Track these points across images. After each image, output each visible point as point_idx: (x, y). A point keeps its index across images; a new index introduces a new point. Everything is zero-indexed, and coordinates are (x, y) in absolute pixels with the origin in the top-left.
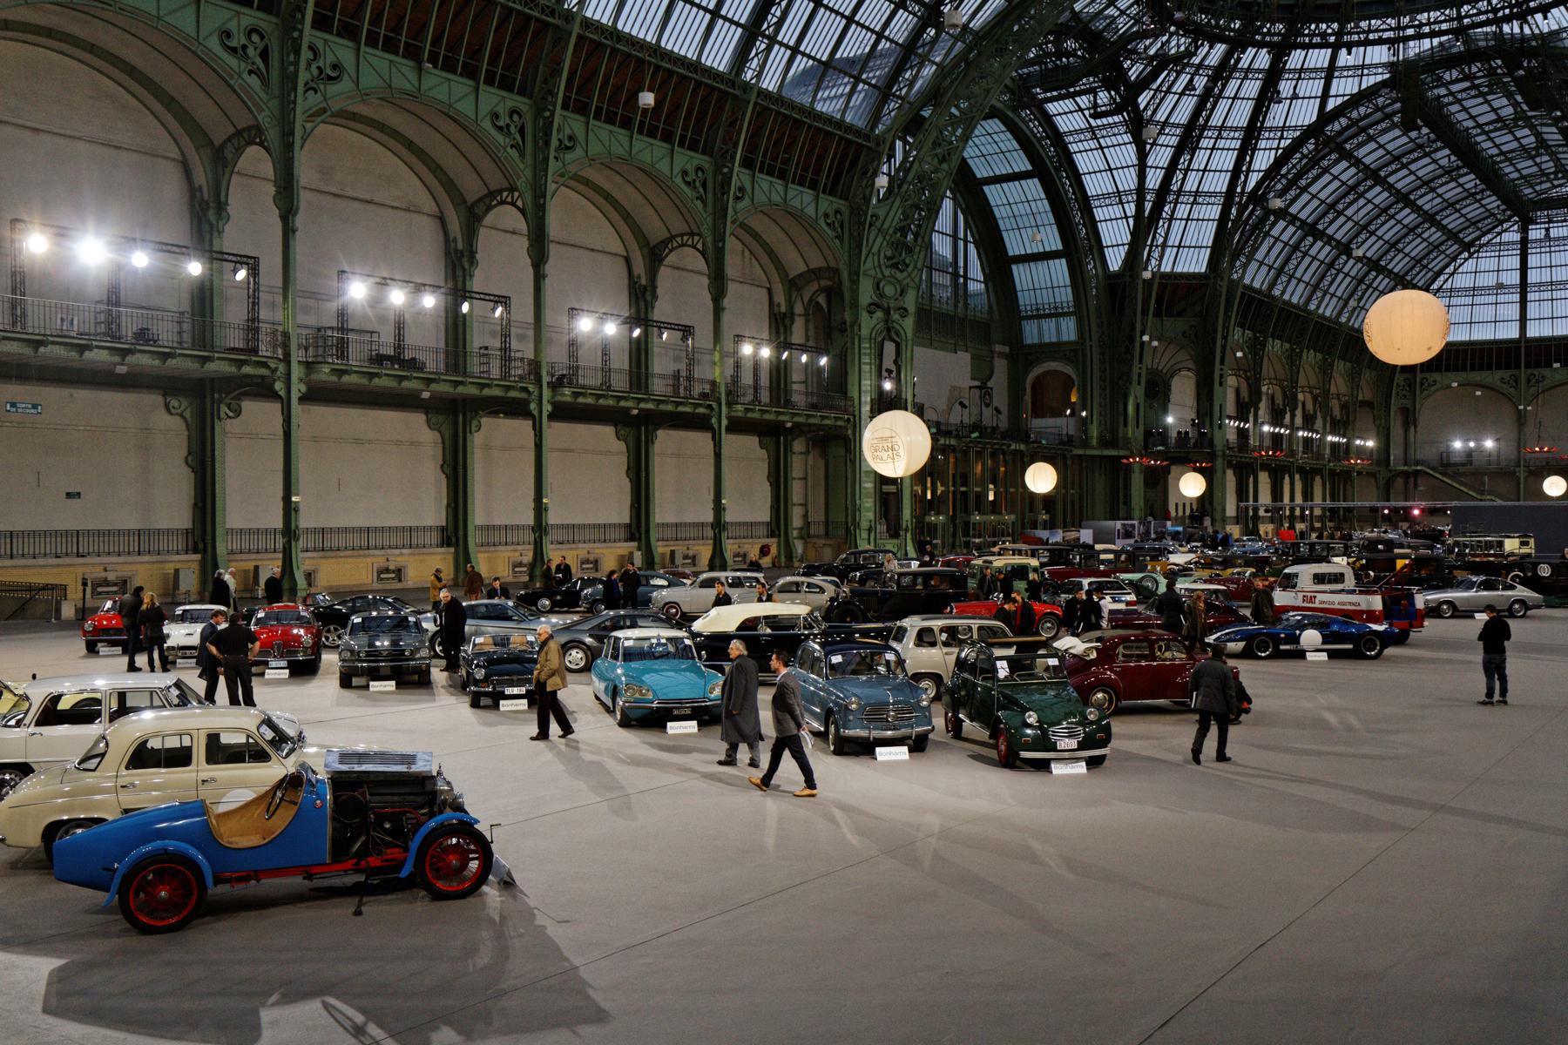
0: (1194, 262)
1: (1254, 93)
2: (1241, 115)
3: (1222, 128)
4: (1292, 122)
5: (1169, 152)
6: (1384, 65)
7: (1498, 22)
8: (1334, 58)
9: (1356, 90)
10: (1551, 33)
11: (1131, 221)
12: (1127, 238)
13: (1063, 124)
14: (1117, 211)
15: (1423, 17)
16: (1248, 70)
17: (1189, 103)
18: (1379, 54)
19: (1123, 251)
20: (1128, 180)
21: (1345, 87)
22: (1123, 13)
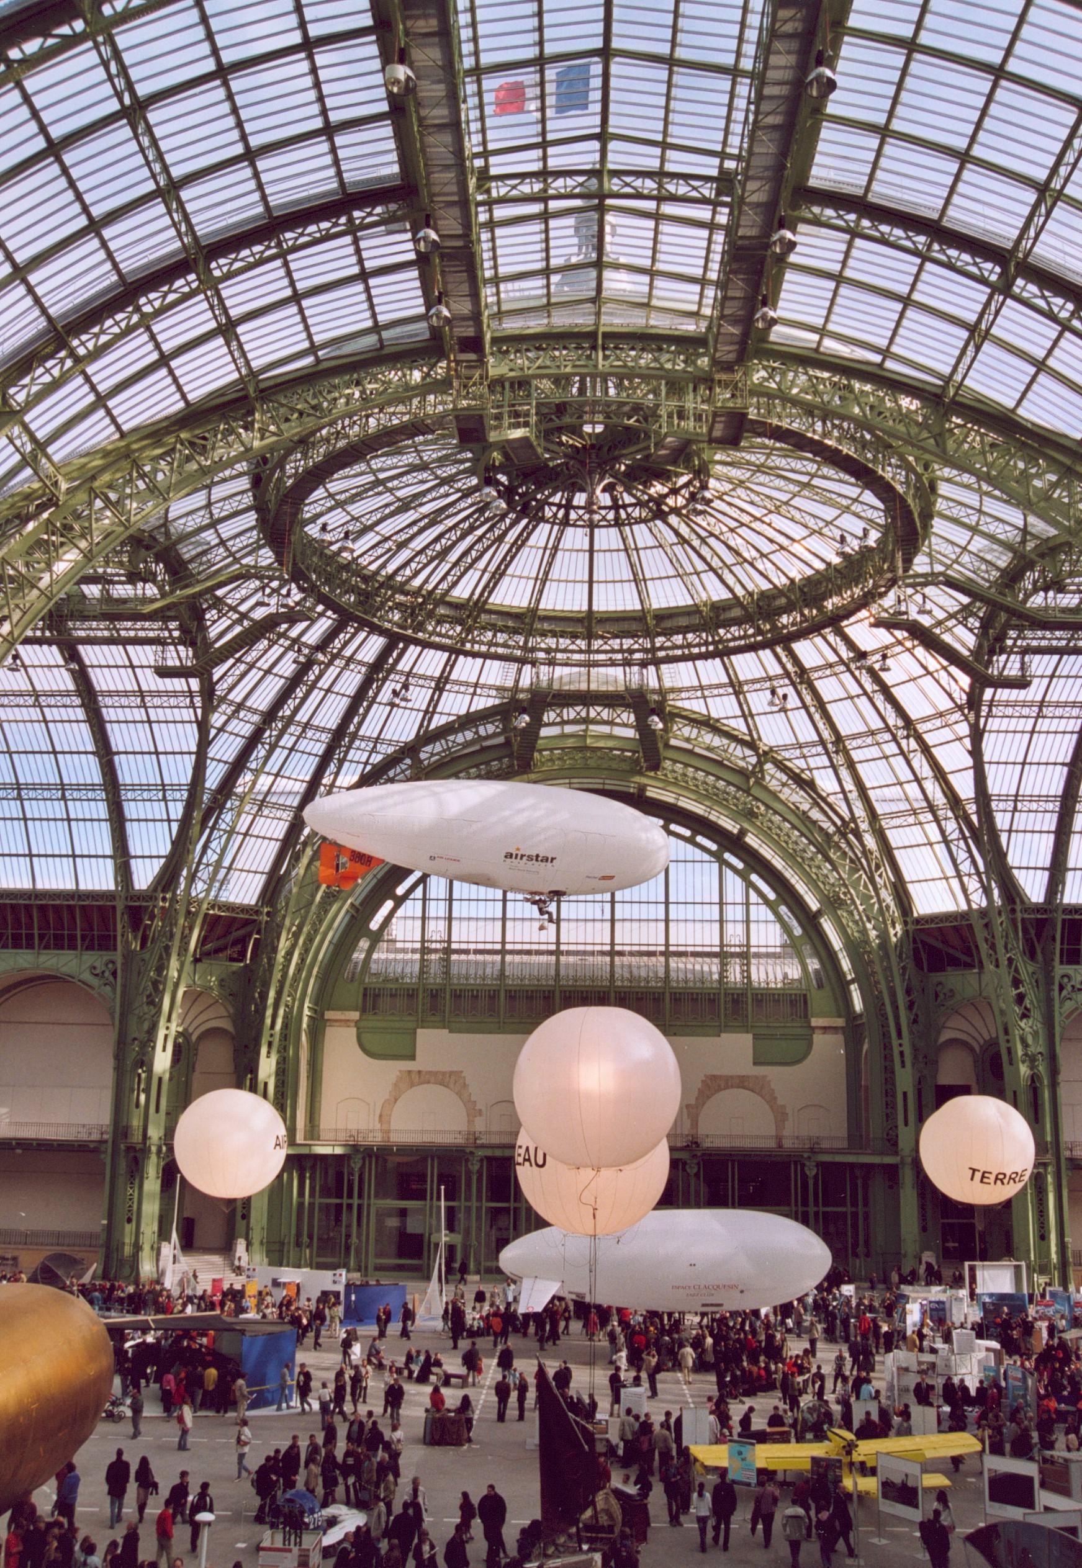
0: (244, 890)
1: (351, 690)
2: (331, 714)
3: (307, 725)
4: (387, 735)
5: (237, 744)
6: (498, 689)
7: (627, 663)
8: (450, 665)
9: (463, 712)
10: (672, 690)
11: (175, 826)
12: (165, 848)
13: (101, 680)
14: (157, 810)
15: (551, 642)
16: (350, 660)
17: (271, 688)
18: (497, 673)
19: (157, 865)
20: (181, 771)
21: (454, 705)
22: (222, 543)
